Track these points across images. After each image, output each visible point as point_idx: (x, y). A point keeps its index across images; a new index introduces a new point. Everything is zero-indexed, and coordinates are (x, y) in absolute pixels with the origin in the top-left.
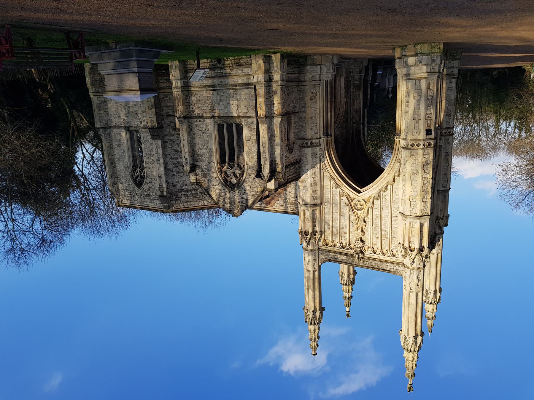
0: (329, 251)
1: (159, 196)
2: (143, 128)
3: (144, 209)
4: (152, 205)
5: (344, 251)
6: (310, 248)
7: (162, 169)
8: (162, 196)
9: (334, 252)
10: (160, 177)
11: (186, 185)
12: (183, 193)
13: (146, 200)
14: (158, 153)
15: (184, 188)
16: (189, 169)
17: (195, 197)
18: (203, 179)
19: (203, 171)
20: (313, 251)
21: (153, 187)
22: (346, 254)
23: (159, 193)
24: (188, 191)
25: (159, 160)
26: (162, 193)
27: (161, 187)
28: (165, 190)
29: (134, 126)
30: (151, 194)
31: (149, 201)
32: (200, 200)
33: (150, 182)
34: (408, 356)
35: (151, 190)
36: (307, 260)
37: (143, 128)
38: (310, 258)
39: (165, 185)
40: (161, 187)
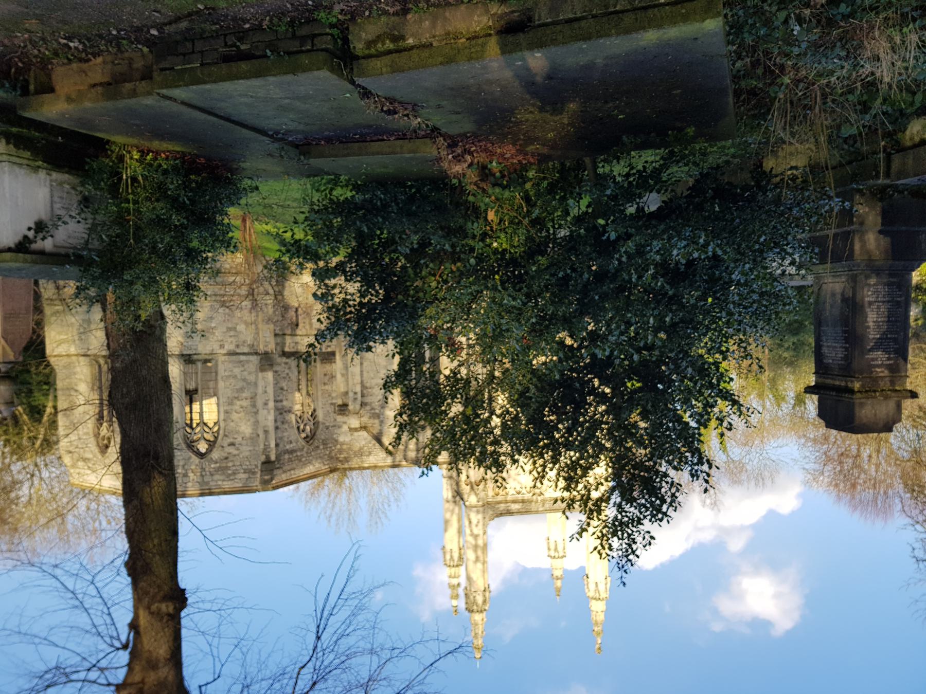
0: (500, 502)
1: (263, 463)
2: (225, 355)
3: (211, 494)
4: (227, 485)
5: (520, 497)
6: (481, 503)
7: (271, 417)
8: (267, 462)
9: (506, 502)
10: (266, 432)
11: (291, 442)
12: (287, 456)
13: (216, 477)
14: (266, 392)
15: (288, 447)
16: (358, 407)
17: (300, 461)
18: (372, 421)
19: (373, 409)
20: (483, 506)
21: (236, 452)
22: (523, 502)
23: (263, 458)
24: (291, 452)
25: (266, 404)
26: (268, 457)
27: (266, 447)
28: (274, 452)
29: (204, 352)
30: (230, 464)
31: (222, 478)
32: (305, 465)
33: (232, 444)
34: (598, 608)
35: (231, 458)
36: (474, 521)
37: (225, 355)
38: (480, 516)
39: (273, 445)
40: (266, 447)
